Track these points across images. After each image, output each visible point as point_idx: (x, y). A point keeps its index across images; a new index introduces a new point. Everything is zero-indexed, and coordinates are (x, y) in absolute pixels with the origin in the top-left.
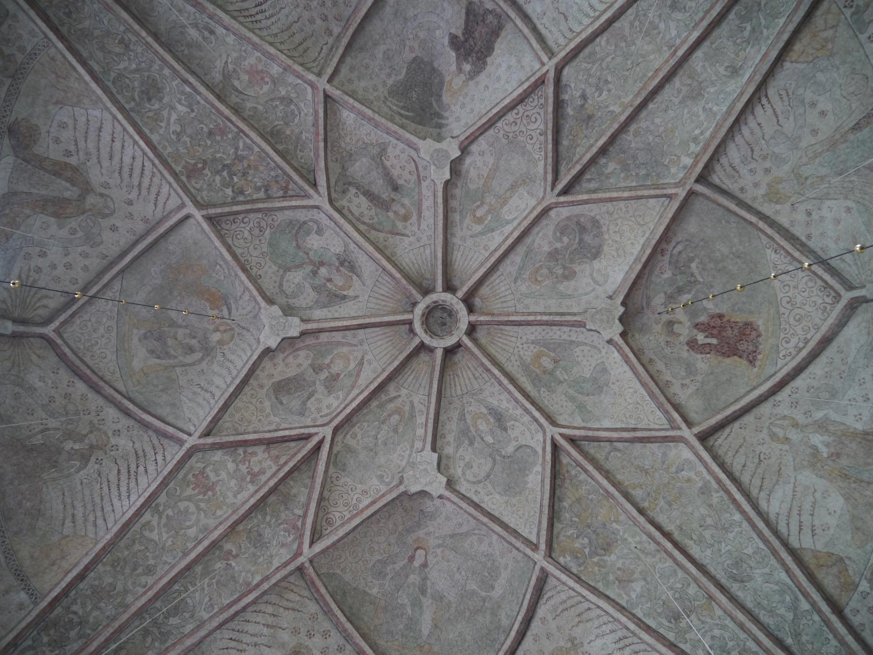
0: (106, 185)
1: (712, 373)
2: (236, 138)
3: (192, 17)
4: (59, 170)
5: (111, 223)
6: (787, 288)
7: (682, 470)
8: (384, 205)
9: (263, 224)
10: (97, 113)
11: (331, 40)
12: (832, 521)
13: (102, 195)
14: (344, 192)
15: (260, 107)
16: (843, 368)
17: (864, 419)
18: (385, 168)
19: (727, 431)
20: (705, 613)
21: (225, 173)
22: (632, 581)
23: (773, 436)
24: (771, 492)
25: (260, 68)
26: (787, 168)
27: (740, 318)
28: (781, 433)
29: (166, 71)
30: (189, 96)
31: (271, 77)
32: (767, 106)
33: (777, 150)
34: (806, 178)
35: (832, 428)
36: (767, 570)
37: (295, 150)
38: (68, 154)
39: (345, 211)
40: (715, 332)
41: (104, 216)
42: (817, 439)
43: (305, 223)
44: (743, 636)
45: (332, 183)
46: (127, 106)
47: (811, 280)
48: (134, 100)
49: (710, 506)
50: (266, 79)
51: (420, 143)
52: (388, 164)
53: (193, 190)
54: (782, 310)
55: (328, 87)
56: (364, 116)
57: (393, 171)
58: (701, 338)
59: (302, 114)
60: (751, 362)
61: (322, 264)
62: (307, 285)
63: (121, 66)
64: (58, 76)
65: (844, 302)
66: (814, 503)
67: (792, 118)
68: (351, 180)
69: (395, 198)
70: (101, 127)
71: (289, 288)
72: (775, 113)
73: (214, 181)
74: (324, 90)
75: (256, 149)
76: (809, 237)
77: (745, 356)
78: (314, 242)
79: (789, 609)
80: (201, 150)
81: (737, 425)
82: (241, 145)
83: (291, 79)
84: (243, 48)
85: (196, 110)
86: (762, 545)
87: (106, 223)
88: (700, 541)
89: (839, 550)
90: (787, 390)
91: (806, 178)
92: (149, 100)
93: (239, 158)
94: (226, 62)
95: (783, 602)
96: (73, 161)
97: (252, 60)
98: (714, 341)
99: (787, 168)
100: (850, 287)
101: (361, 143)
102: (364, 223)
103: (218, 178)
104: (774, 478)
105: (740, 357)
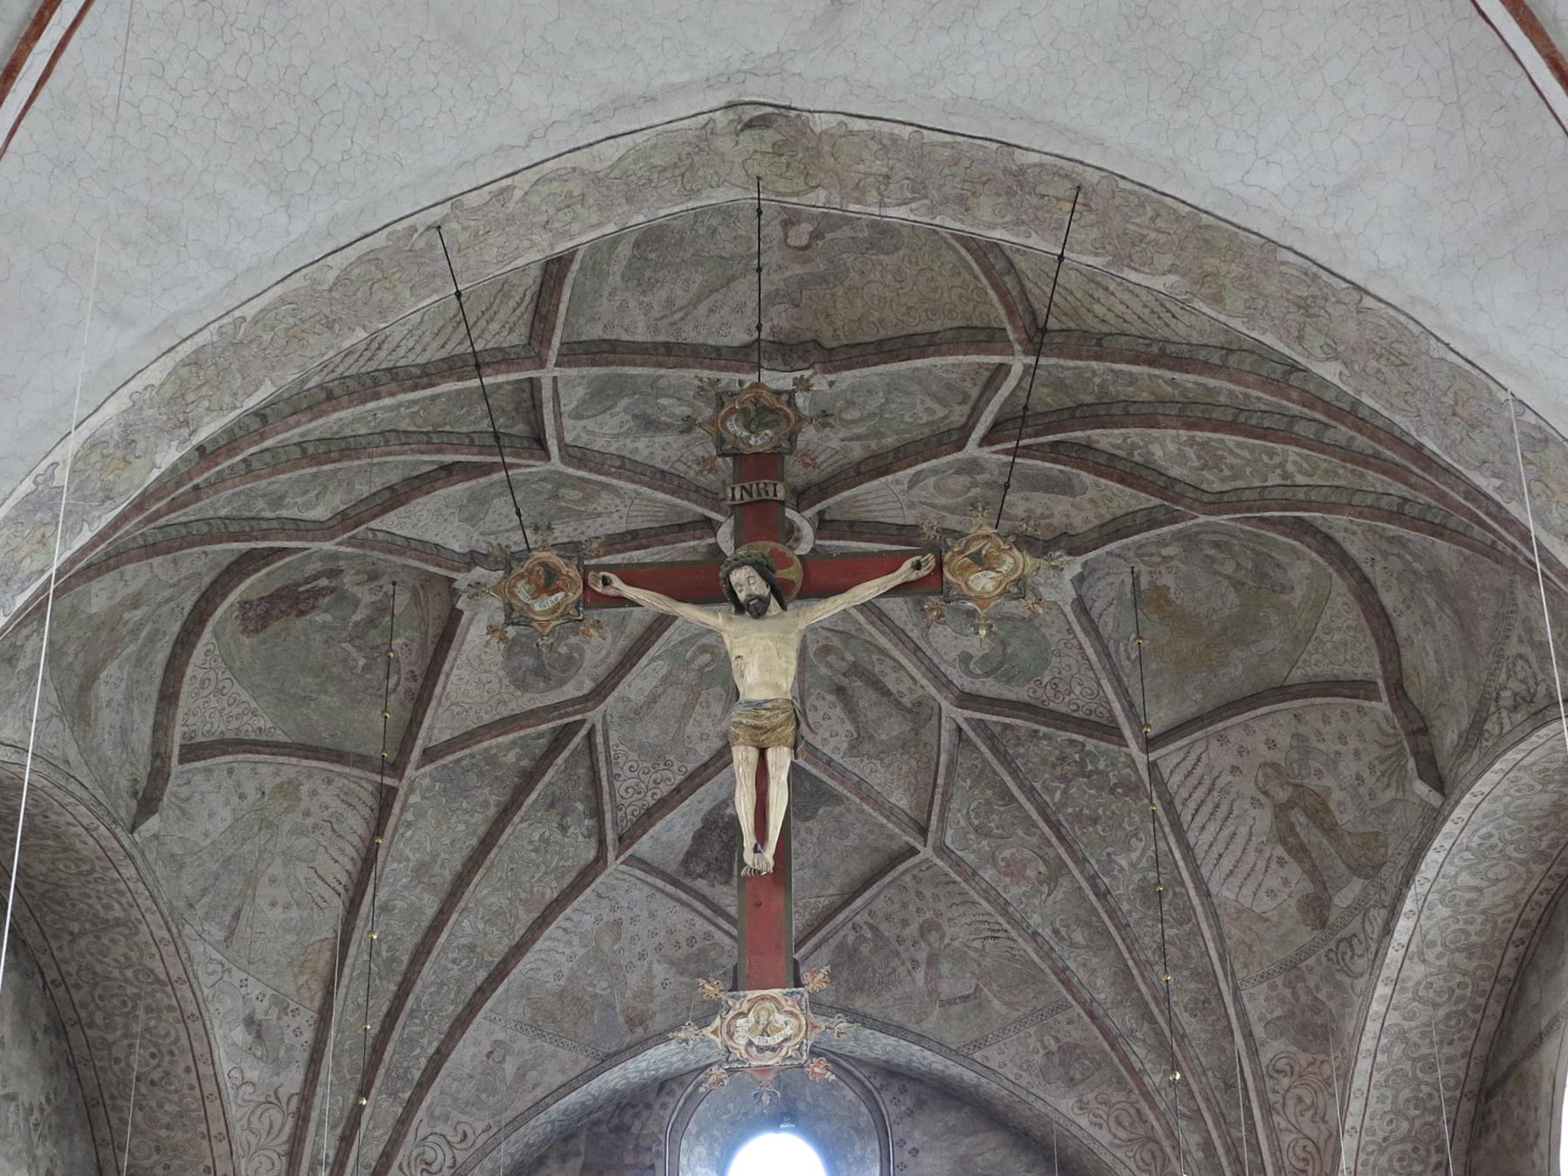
0: (1255, 803)
3: (1072, 955)
6: (231, 701)
8: (856, 670)
14: (920, 704)
18: (854, 721)
26: (286, 827)
30: (1108, 873)
32: (334, 884)
33: (305, 840)
34: (260, 829)
45: (935, 718)
47: (208, 732)
52: (849, 727)
54: (227, 674)
57: (843, 716)
63: (1175, 931)
67: (303, 882)
68: (907, 715)
69: (841, 677)
70: (1228, 876)
72: (323, 880)
74: (925, 846)
91: (260, 829)
94: (1049, 895)
99: (286, 827)
101: (887, 761)
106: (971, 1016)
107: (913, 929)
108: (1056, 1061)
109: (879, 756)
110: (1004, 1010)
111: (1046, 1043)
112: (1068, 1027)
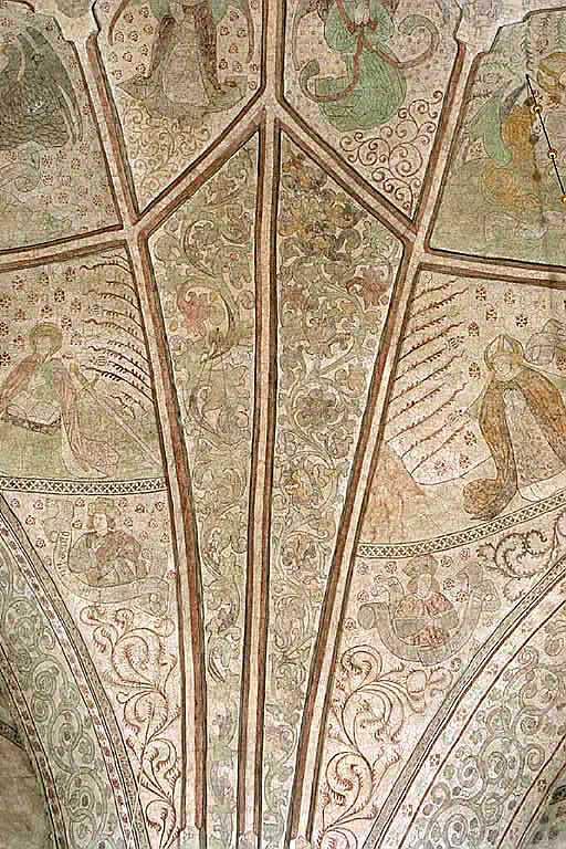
0: (474, 370)
2: (288, 273)
4: (498, 434)
5: (519, 328)
9: (364, 151)
10: (395, 445)
11: (75, 264)
13: (491, 367)
14: (234, 85)
15: (226, 277)
21: (342, 250)
25: (181, 317)
29: (281, 411)
31: (180, 295)
37: (238, 192)
38: (469, 439)
39: (256, 60)
41: (514, 343)
43: (318, 99)
45: (237, 110)
46: (359, 421)
48: (345, 420)
50: (188, 299)
51: (80, 45)
52: (147, 62)
53: (395, 271)
55: (127, 223)
56: (120, 147)
59: (190, 222)
61: (352, 27)
62: (397, 20)
63: (320, 461)
64: (389, 513)
71: (421, 41)
73: (362, 256)
75: (279, 239)
78: (333, 65)
80: (338, 302)
82: (290, 261)
83: (160, 272)
84: (178, 353)
85: (297, 345)
87: (520, 334)
92: (330, 404)
93: (310, 249)
94: (212, 358)
96: (474, 427)
97: (182, 332)
102: (250, 21)
103: (356, 254)
106: (29, 448)
107: (24, 327)
108: (96, 546)
109: (153, 111)
110: (70, 462)
111: (96, 521)
112: (133, 515)
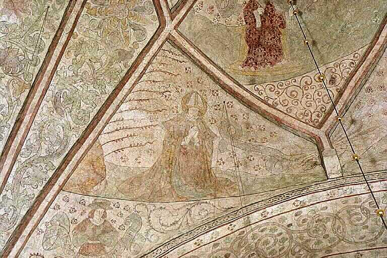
1: (228, 31)
7: (134, 30)
12: (131, 163)
16: (259, 140)
17: (221, 167)
19: (181, 58)
20: (16, 86)
22: (16, 13)
23: (186, 99)
24: (140, 109)
27: (284, 41)
28: (191, 103)
35: (207, 143)
36: (73, 125)
40: (267, 23)
42: (194, 133)
44: (12, 123)
49: (111, 63)
54: (298, 79)
58: (260, 11)
60: (246, 63)
65: (316, 131)
66: (141, 145)
76: (369, 90)
77: (251, 56)
79: (48, 151)
81: (189, 64)
86: (92, 115)
88: (77, 63)
89: (110, 175)
90: (229, 98)
95: (52, 145)
98: (258, 25)
100: (328, 135)
104: (152, 109)
105: (249, 52)
